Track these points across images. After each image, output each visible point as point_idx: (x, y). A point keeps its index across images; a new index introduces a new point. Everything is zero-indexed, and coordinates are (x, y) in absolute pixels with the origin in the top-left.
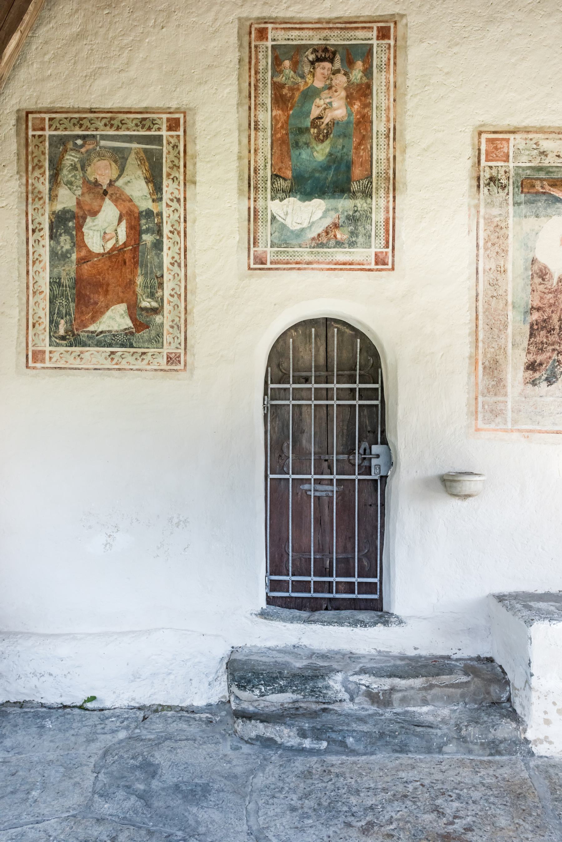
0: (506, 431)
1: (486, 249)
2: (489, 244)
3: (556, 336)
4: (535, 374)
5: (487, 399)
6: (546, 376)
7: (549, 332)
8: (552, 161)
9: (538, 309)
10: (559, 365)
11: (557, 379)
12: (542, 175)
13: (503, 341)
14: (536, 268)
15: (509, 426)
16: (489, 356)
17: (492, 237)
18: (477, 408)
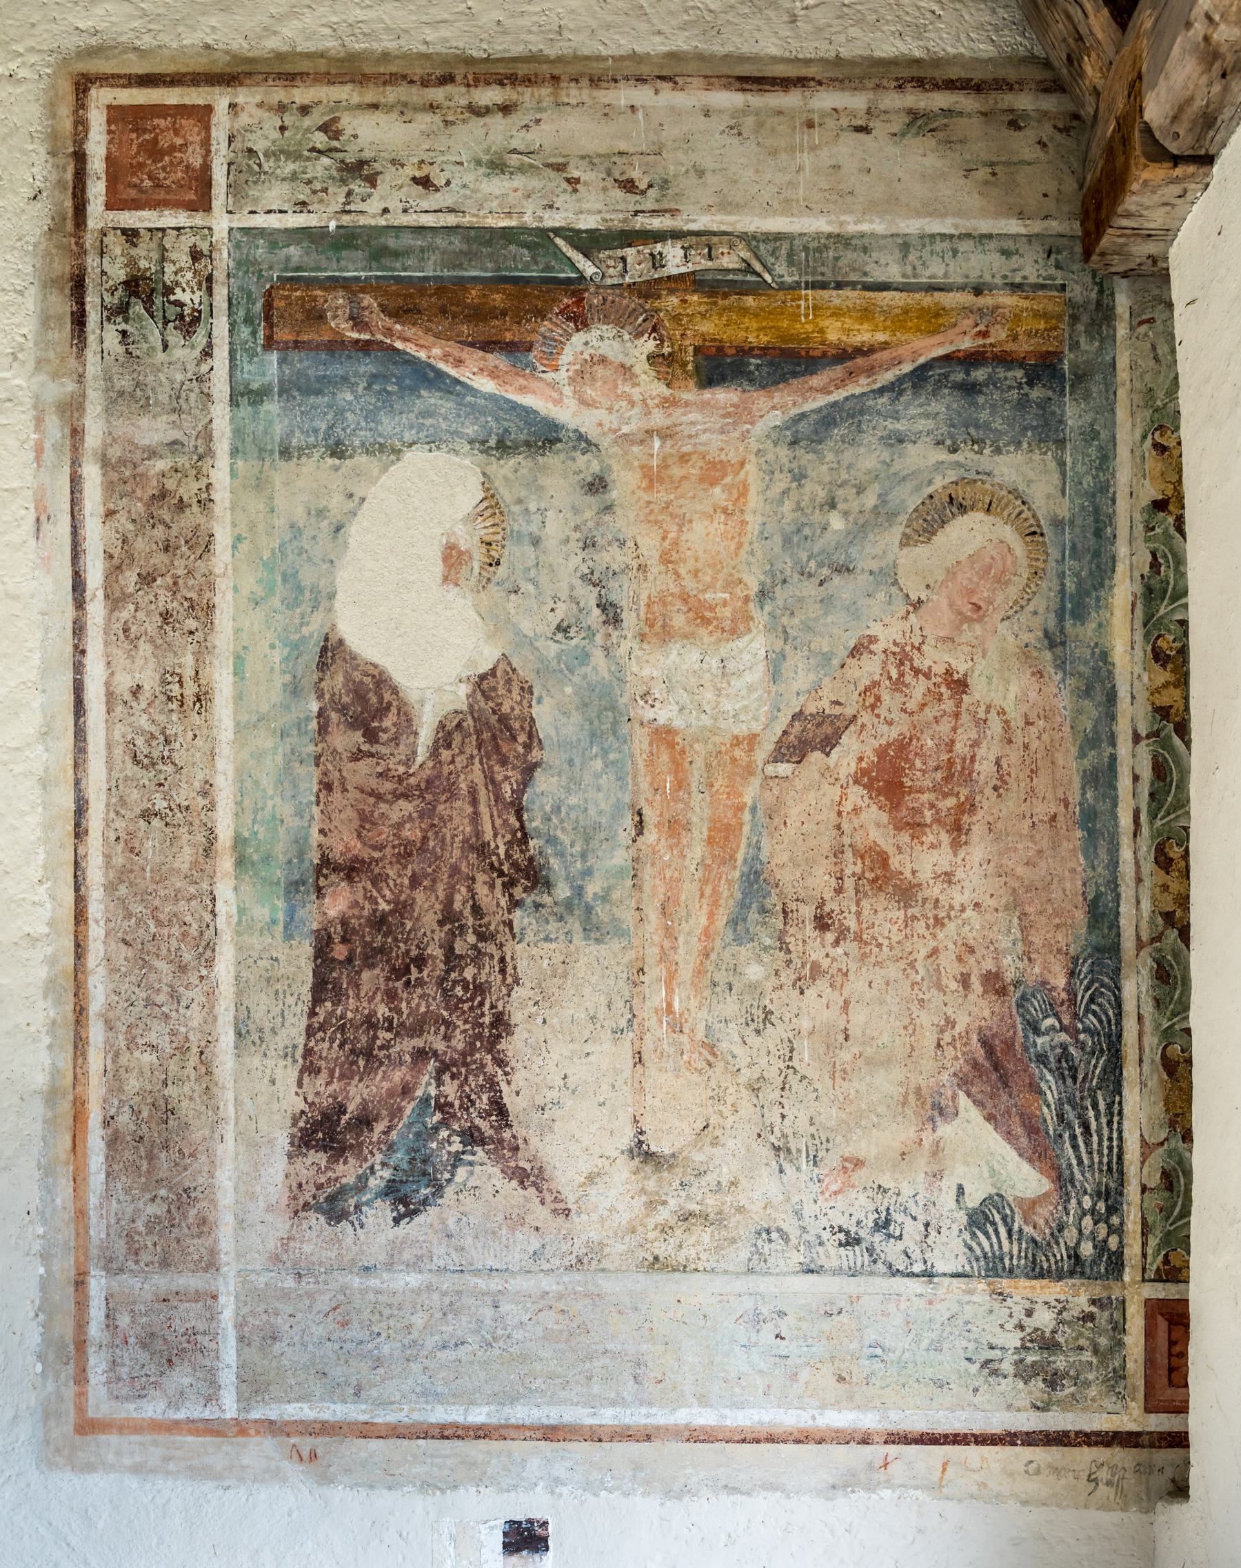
0: (212, 1429)
1: (115, 601)
2: (130, 579)
3: (431, 990)
4: (340, 1168)
5: (131, 1283)
6: (387, 1174)
7: (400, 972)
8: (394, 205)
9: (351, 870)
10: (444, 1123)
11: (439, 1190)
12: (355, 268)
13: (195, 1017)
14: (336, 682)
15: (229, 1406)
16: (133, 1084)
17: (140, 544)
18: (81, 1324)
